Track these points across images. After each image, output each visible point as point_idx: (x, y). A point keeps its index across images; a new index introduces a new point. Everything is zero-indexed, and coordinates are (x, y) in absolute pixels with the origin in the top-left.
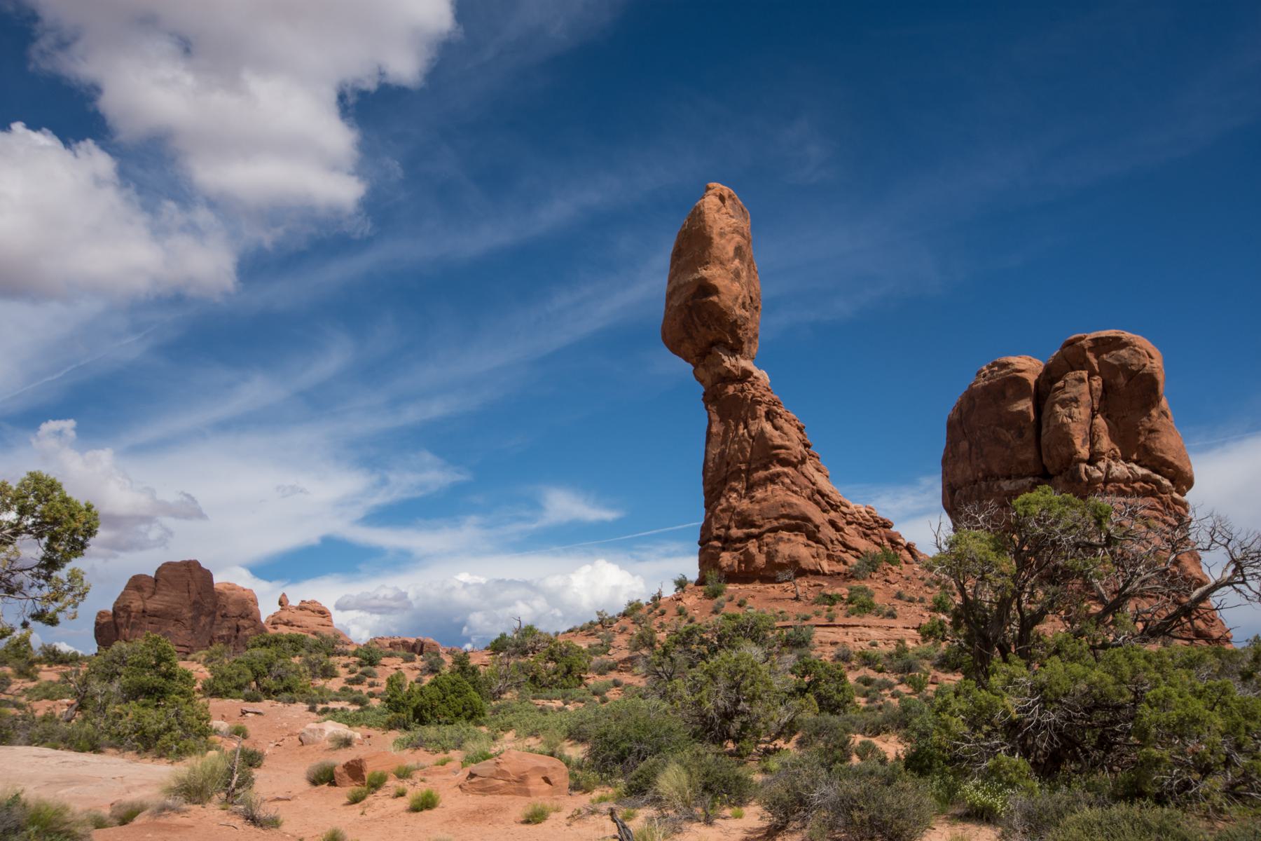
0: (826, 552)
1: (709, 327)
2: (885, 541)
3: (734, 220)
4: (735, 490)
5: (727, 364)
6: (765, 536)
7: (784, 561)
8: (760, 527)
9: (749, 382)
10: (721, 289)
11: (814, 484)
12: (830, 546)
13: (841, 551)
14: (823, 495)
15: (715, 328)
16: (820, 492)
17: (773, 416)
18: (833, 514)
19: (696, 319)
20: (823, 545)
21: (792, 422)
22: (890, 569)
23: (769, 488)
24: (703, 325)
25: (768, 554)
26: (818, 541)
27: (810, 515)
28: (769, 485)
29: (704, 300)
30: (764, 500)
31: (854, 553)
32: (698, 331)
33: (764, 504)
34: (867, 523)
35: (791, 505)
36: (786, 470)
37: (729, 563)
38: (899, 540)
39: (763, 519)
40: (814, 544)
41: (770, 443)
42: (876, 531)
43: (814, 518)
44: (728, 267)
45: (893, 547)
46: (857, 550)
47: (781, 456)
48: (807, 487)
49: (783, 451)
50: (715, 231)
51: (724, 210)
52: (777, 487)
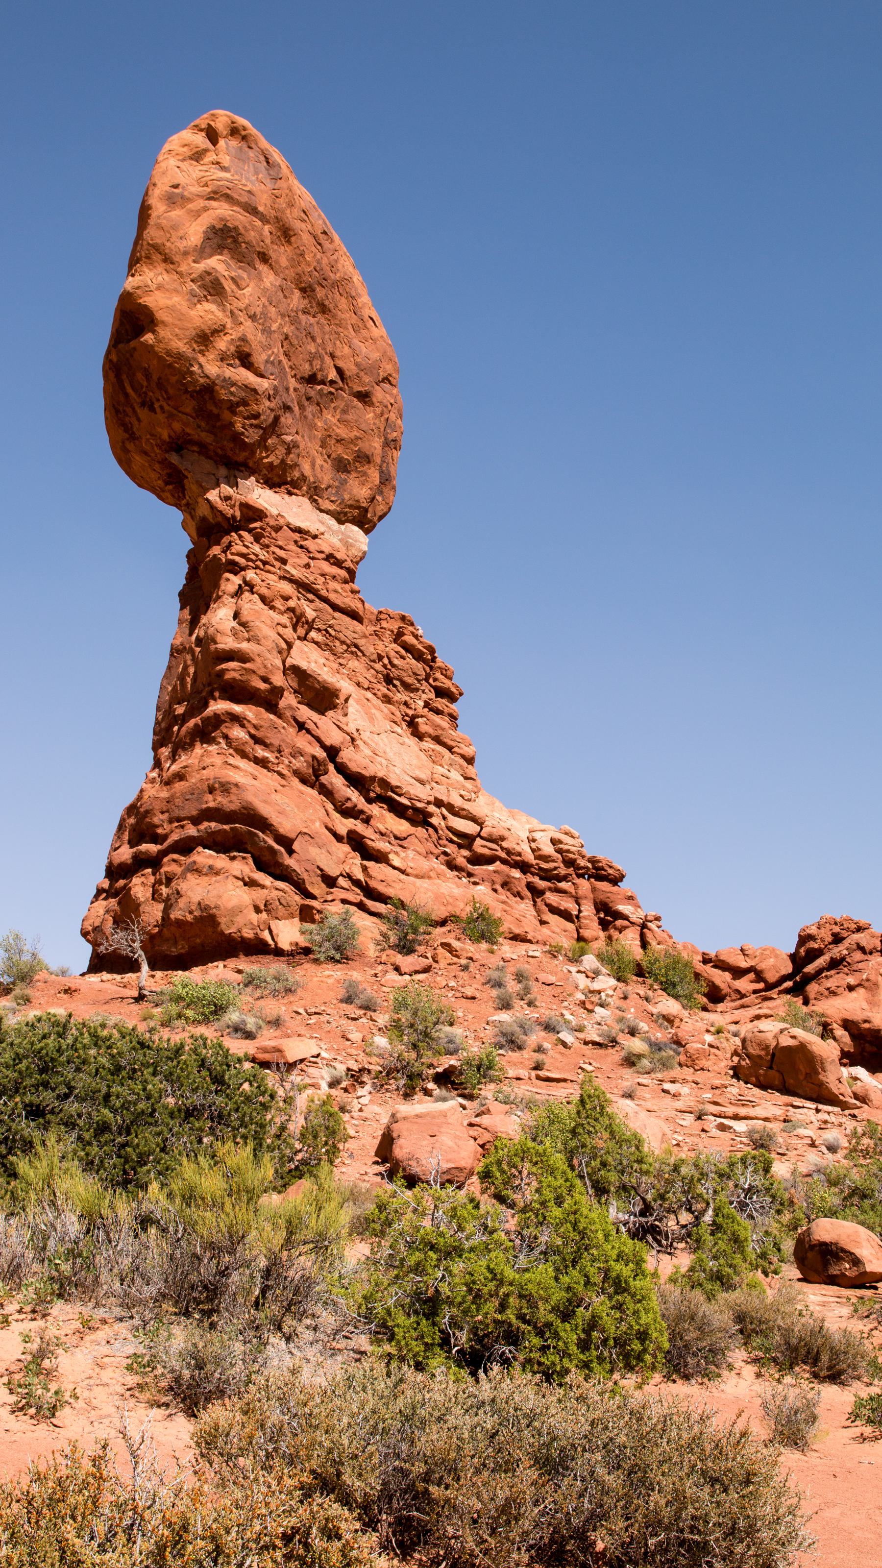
0: (297, 899)
1: (152, 409)
6: (165, 860)
7: (189, 918)
8: (163, 838)
9: (250, 531)
10: (160, 315)
12: (317, 888)
14: (356, 780)
15: (162, 407)
16: (342, 769)
19: (129, 390)
21: (278, 603)
22: (446, 946)
24: (143, 404)
26: (282, 874)
27: (265, 810)
29: (133, 344)
30: (180, 776)
32: (139, 420)
33: (179, 786)
34: (544, 865)
35: (226, 788)
36: (238, 708)
37: (96, 924)
38: (621, 908)
39: (171, 821)
43: (275, 819)
44: (183, 268)
45: (604, 925)
47: (228, 676)
48: (297, 753)
51: (211, 157)
52: (213, 748)
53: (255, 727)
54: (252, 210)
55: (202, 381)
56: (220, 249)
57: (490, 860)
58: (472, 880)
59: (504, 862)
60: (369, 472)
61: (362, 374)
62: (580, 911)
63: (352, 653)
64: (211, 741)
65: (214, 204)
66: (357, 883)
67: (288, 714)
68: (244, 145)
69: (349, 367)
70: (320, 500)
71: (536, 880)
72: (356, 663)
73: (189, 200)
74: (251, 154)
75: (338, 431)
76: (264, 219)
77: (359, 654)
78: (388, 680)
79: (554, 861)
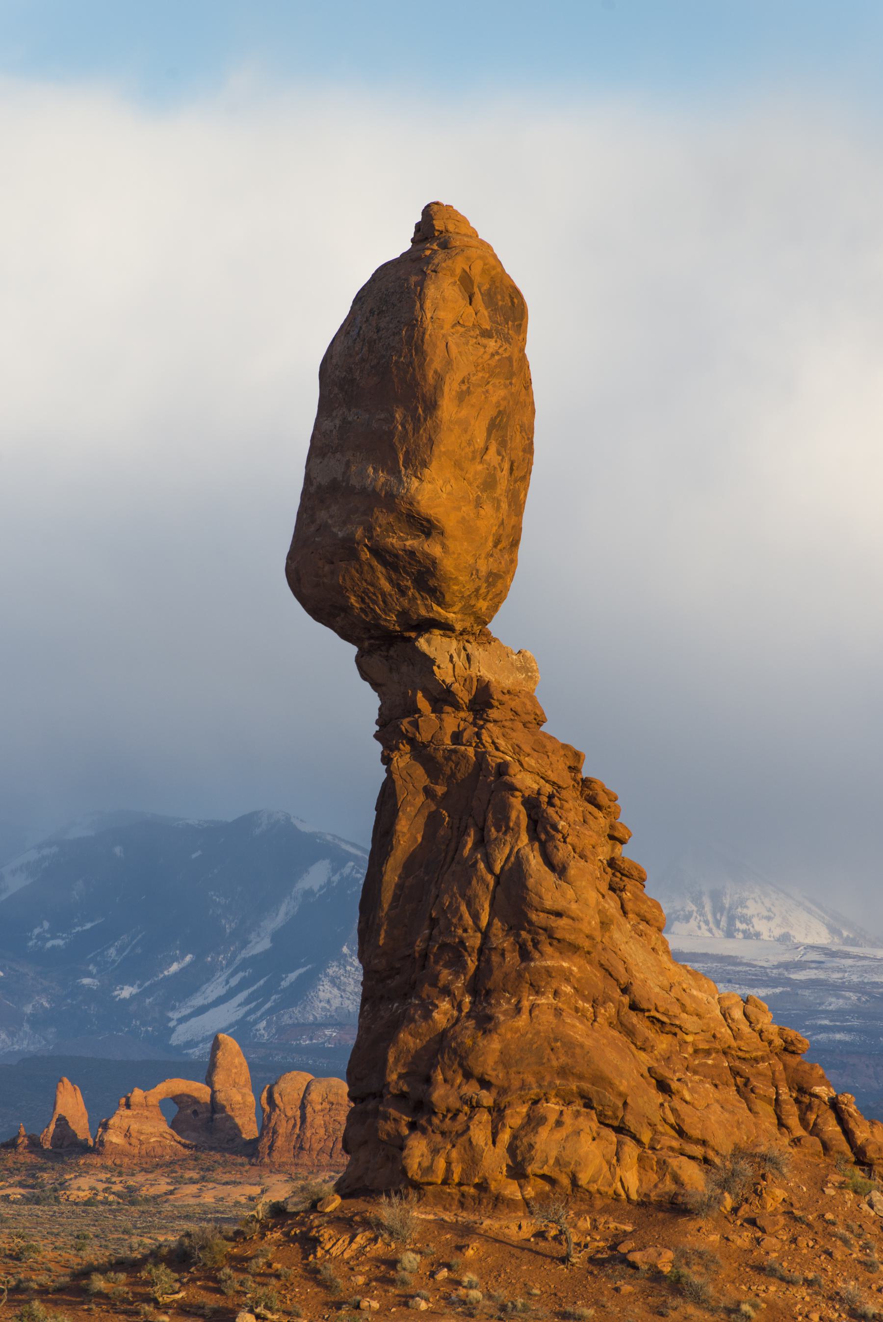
2: (784, 1090)
3: (492, 344)
4: (446, 991)
5: (444, 673)
11: (625, 991)
13: (672, 1149)
15: (429, 609)
16: (634, 1007)
17: (547, 833)
18: (663, 1043)
20: (634, 1137)
23: (526, 1004)
25: (512, 1150)
28: (525, 994)
31: (698, 1151)
35: (570, 1046)
37: (426, 1164)
38: (817, 1090)
40: (613, 1136)
41: (535, 899)
42: (762, 1066)
44: (470, 476)
46: (704, 1143)
49: (563, 922)
50: (446, 389)
52: (543, 1001)
57: (708, 1053)
62: (777, 1093)
64: (537, 993)
65: (490, 387)
66: (672, 1126)
71: (737, 1063)
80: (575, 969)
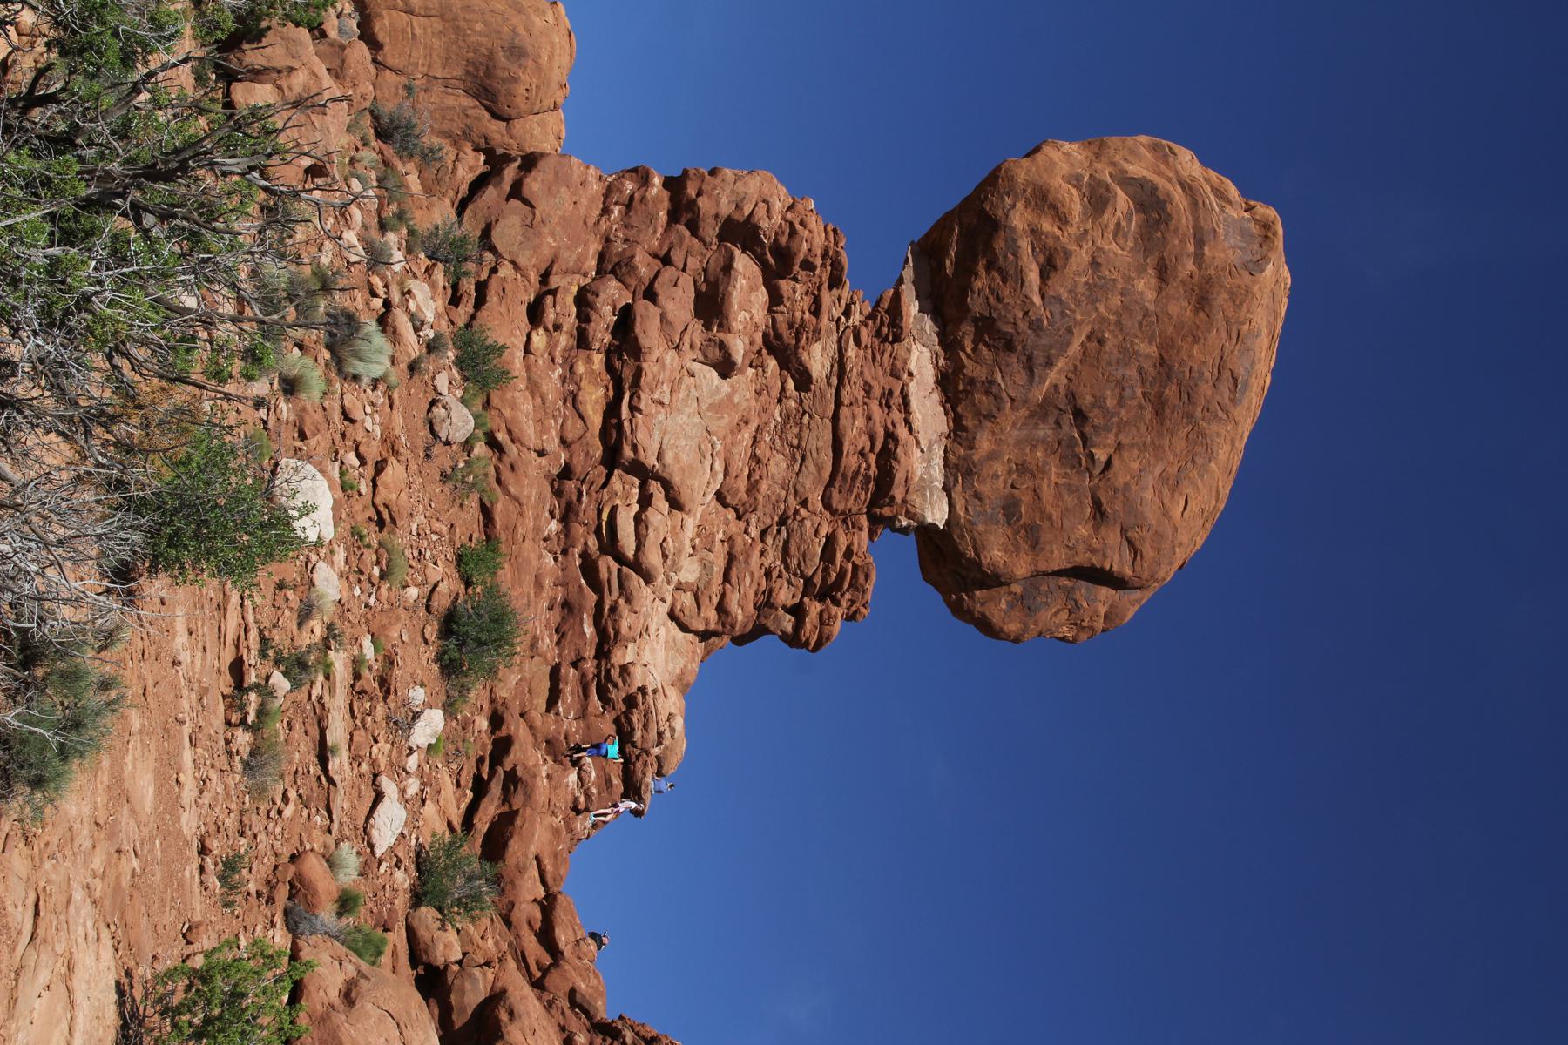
53: (643, 198)
54: (1200, 243)
55: (1000, 213)
56: (1141, 207)
58: (560, 558)
59: (599, 605)
60: (1023, 555)
61: (1120, 495)
63: (793, 456)
67: (673, 237)
68: (1260, 239)
69: (1120, 476)
70: (959, 487)
72: (784, 465)
73: (1167, 163)
74: (1256, 247)
75: (1045, 486)
76: (1199, 258)
77: (797, 467)
78: (783, 521)
79: (624, 682)
80: (655, 191)
